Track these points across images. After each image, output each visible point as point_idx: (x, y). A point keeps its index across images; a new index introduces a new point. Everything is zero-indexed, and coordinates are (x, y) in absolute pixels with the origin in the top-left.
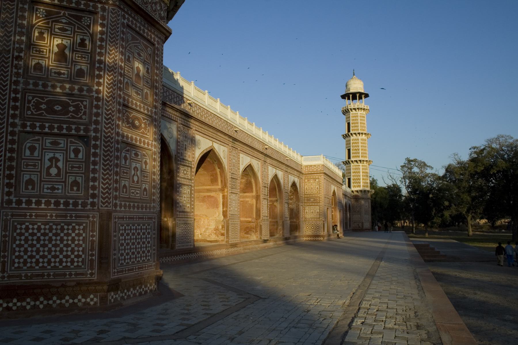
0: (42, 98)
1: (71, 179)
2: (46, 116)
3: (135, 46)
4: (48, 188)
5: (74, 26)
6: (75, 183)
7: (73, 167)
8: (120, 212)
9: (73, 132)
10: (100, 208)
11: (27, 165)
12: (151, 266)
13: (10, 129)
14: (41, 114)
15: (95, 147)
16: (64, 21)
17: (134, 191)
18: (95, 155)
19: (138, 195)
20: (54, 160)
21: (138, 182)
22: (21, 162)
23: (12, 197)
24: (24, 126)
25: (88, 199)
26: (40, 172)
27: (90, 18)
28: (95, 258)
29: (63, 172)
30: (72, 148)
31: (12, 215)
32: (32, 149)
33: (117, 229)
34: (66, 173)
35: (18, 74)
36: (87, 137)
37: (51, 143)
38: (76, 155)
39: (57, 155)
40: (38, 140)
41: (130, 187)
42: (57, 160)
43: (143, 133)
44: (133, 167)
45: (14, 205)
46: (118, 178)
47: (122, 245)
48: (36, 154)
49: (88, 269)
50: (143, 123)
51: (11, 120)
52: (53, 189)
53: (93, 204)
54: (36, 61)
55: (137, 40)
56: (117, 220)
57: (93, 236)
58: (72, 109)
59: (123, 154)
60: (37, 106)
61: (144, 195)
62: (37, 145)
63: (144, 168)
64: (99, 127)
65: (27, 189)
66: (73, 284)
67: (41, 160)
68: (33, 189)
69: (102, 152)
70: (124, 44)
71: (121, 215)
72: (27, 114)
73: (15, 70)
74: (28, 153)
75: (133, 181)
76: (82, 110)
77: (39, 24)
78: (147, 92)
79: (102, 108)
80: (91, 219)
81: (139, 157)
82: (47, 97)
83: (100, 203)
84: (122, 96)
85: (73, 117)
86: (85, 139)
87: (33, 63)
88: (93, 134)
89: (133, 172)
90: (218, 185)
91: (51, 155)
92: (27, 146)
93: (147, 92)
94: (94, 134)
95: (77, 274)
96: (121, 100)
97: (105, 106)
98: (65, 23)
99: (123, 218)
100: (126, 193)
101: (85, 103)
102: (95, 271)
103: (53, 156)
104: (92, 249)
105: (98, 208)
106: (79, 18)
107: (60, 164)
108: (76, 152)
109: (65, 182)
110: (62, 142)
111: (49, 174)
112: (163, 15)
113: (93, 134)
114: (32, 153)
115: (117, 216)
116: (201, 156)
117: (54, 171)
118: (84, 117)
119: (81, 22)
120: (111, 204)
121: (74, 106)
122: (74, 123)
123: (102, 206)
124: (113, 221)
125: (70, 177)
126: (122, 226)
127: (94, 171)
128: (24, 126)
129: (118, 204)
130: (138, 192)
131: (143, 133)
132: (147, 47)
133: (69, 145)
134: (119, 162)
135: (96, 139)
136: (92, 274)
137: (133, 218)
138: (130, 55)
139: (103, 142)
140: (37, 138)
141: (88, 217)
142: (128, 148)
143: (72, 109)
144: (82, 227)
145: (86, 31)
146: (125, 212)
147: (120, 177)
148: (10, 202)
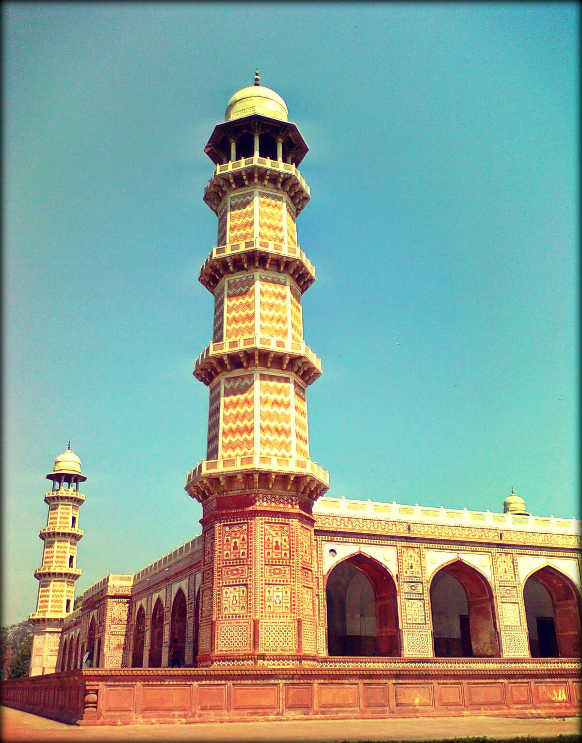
1: (241, 605)
6: (243, 607)
9: (241, 583)
12: (293, 650)
15: (250, 588)
18: (250, 592)
28: (252, 642)
31: (220, 623)
42: (236, 597)
43: (283, 576)
48: (228, 595)
52: (234, 610)
53: (250, 616)
58: (240, 572)
60: (227, 573)
62: (228, 591)
66: (242, 654)
86: (246, 585)
90: (486, 596)
95: (245, 650)
102: (252, 648)
106: (241, 527)
107: (237, 598)
108: (243, 591)
110: (237, 588)
111: (233, 604)
113: (249, 582)
117: (234, 602)
122: (242, 578)
124: (260, 624)
127: (250, 600)
131: (283, 576)
135: (250, 584)
136: (250, 650)
137: (276, 623)
141: (248, 622)
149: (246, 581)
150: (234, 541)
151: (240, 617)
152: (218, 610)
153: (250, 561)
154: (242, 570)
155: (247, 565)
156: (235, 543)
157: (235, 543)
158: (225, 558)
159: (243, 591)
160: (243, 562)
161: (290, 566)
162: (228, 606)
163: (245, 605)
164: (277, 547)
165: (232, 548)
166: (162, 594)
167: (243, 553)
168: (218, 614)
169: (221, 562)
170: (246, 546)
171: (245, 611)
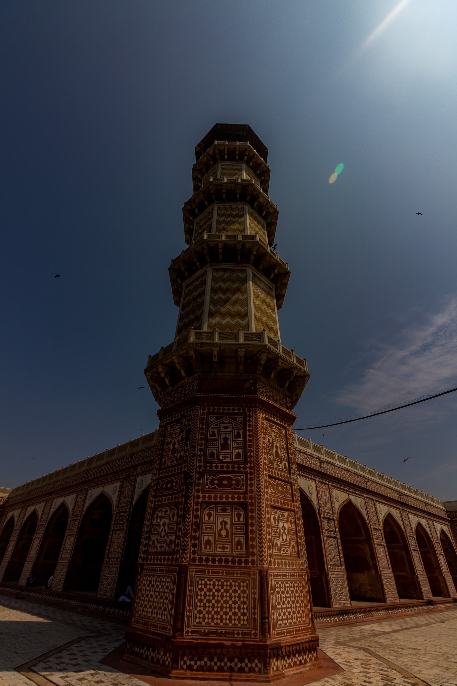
0: (215, 476)
1: (237, 539)
2: (217, 489)
3: (272, 431)
4: (220, 548)
5: (233, 424)
6: (239, 543)
7: (237, 529)
8: (275, 569)
10: (259, 566)
11: (206, 528)
13: (196, 500)
14: (214, 488)
16: (226, 422)
17: (284, 548)
19: (288, 552)
20: (224, 523)
21: (286, 539)
22: (202, 526)
23: (196, 556)
24: (204, 497)
25: (249, 557)
26: (215, 533)
27: (242, 418)
28: (257, 617)
29: (230, 533)
30: (236, 513)
32: (209, 515)
33: (273, 587)
34: (233, 534)
35: (200, 461)
36: (246, 504)
37: (221, 510)
38: (239, 519)
39: (226, 519)
40: (213, 508)
41: (281, 545)
42: (226, 523)
44: (281, 527)
45: (197, 563)
46: (270, 537)
47: (279, 603)
48: (212, 518)
49: (252, 629)
50: (284, 488)
51: (196, 494)
52: (224, 548)
54: (211, 451)
55: (274, 426)
56: (272, 577)
57: (254, 593)
58: (234, 482)
59: (273, 516)
61: (293, 552)
62: (212, 512)
63: (290, 527)
64: (253, 495)
65: (206, 548)
67: (215, 524)
68: (210, 548)
69: (257, 515)
70: (264, 431)
71: (276, 572)
72: (206, 489)
73: (199, 458)
74: (207, 518)
75: (283, 540)
76: (241, 482)
77: (212, 426)
78: (285, 463)
79: (254, 479)
80: (252, 576)
81: (285, 517)
82: (218, 475)
83: (259, 561)
84: (267, 469)
85: (235, 489)
86: (244, 506)
87: (209, 452)
88: (249, 501)
89: (282, 531)
91: (222, 519)
92: (206, 513)
93: (285, 464)
94: (250, 501)
96: (267, 473)
97: (256, 478)
98: (227, 423)
99: (277, 575)
100: (278, 551)
101: (242, 477)
103: (223, 520)
104: (255, 608)
105: (257, 565)
106: (235, 419)
107: (228, 527)
109: (232, 542)
111: (220, 535)
112: (288, 406)
113: (249, 501)
114: (209, 518)
115: (272, 574)
116: (340, 508)
117: (224, 533)
118: (242, 488)
119: (236, 421)
120: (267, 562)
121: (235, 480)
123: (260, 564)
125: (235, 537)
126: (277, 583)
128: (204, 497)
129: (272, 562)
130: (288, 549)
132: (280, 430)
133: (233, 510)
134: (270, 523)
135: (252, 504)
136: (255, 634)
137: (286, 575)
138: (270, 438)
139: (257, 507)
140: (212, 506)
142: (276, 510)
143: (234, 482)
144: (245, 584)
145: (240, 427)
146: (279, 569)
147: (272, 536)
148: (194, 560)
149: (245, 498)
150: (223, 436)
151: (233, 561)
152: (194, 545)
153: (251, 468)
154: (237, 480)
155: (246, 473)
156: (226, 439)
157: (226, 439)
158: (209, 459)
159: (239, 516)
160: (239, 468)
161: (291, 483)
162: (211, 539)
163: (242, 540)
164: (277, 454)
165: (220, 447)
166: (39, 507)
167: (238, 454)
168: (194, 552)
169: (202, 464)
170: (242, 445)
171: (244, 550)
